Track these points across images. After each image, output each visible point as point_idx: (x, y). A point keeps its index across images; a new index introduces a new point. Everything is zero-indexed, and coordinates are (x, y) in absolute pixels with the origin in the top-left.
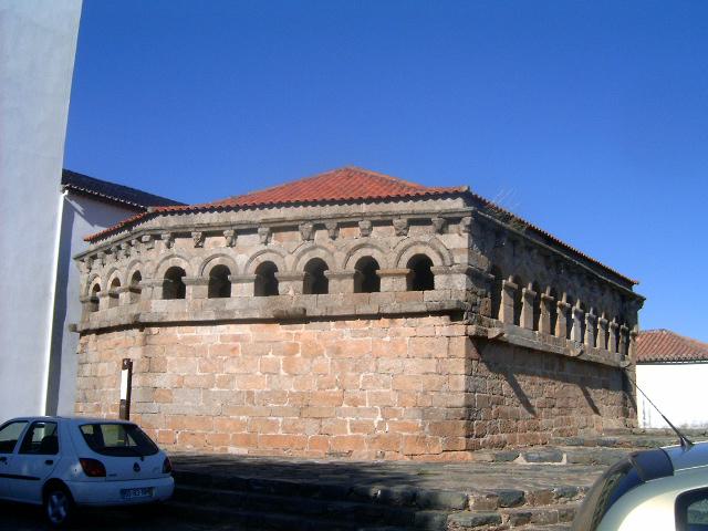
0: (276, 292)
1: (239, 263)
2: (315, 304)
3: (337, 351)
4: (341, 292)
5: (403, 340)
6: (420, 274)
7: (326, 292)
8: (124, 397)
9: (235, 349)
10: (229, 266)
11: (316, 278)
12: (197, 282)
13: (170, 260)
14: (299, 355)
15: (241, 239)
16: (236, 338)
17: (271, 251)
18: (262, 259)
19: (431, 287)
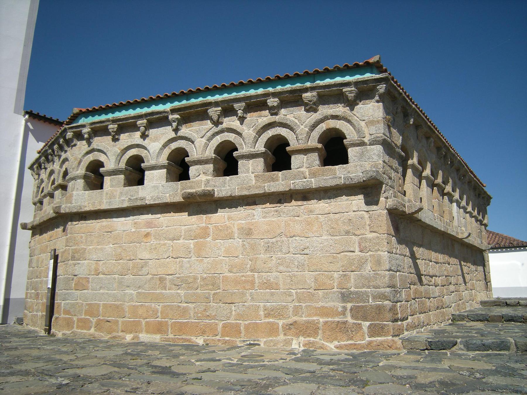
0: (188, 178)
2: (226, 186)
3: (247, 232)
4: (251, 175)
5: (317, 218)
6: (334, 150)
7: (236, 173)
8: (50, 286)
9: (147, 235)
11: (227, 161)
12: (114, 173)
15: (153, 132)
18: (174, 146)
19: (344, 160)
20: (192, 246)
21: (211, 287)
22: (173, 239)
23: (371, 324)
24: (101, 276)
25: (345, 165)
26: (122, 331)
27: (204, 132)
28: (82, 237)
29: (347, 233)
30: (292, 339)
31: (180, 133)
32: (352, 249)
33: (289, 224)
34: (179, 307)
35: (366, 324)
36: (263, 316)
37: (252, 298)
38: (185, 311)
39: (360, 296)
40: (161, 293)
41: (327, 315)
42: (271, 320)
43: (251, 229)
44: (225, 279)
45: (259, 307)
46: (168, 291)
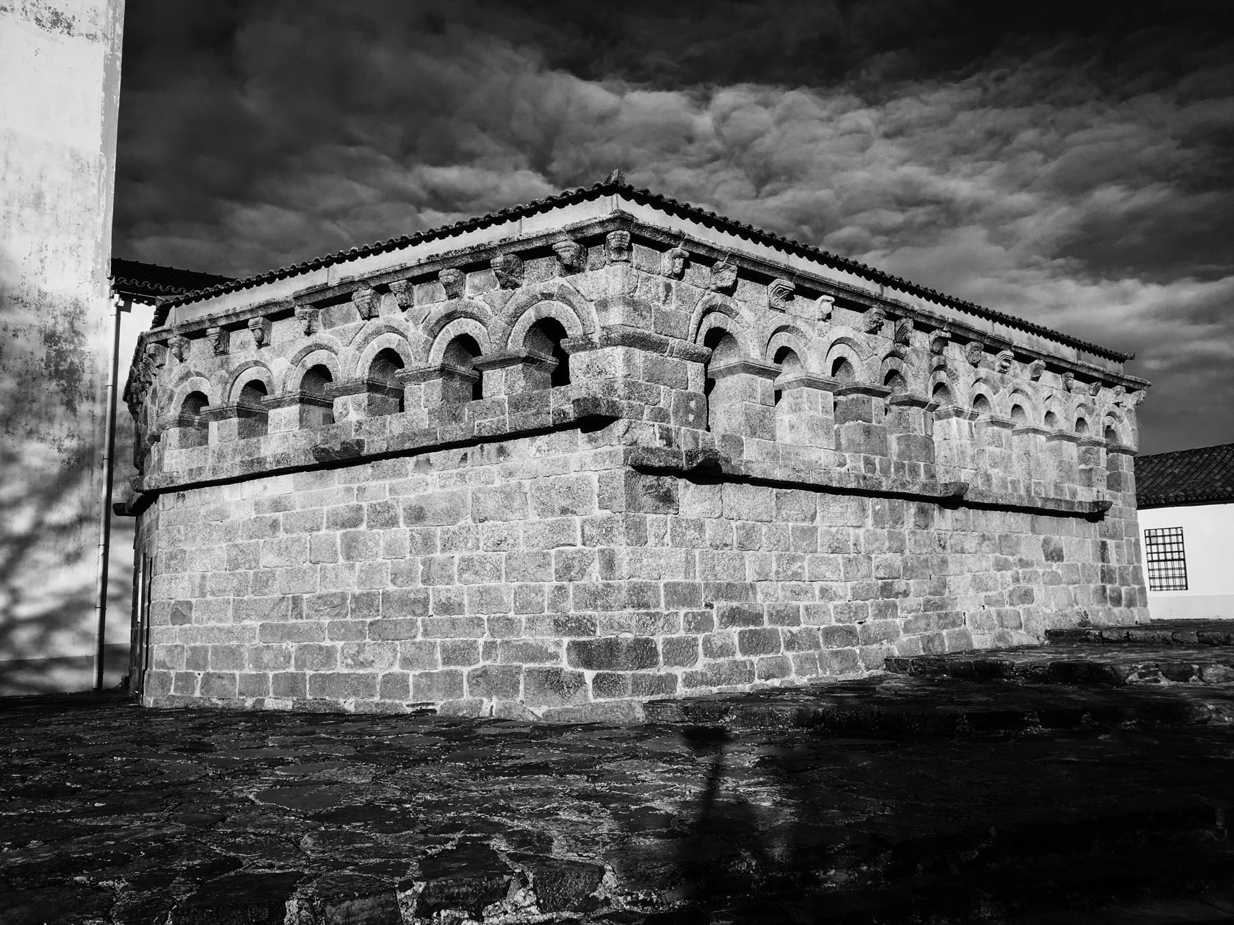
1: (275, 374)
3: (417, 515)
9: (274, 525)
10: (265, 380)
13: (186, 383)
14: (363, 527)
16: (277, 505)
17: (320, 347)
20: (339, 541)
21: (365, 612)
22: (312, 529)
23: (598, 676)
24: (209, 597)
25: (563, 388)
26: (241, 694)
27: (350, 336)
28: (179, 531)
29: (564, 511)
30: (482, 702)
31: (235, 364)
32: (571, 541)
33: (478, 499)
34: (321, 648)
35: (589, 675)
36: (440, 661)
37: (425, 630)
38: (329, 654)
39: (582, 626)
40: (294, 625)
41: (533, 659)
42: (452, 667)
43: (421, 509)
44: (386, 596)
45: (433, 645)
46: (305, 620)
